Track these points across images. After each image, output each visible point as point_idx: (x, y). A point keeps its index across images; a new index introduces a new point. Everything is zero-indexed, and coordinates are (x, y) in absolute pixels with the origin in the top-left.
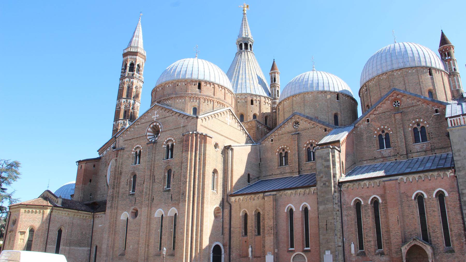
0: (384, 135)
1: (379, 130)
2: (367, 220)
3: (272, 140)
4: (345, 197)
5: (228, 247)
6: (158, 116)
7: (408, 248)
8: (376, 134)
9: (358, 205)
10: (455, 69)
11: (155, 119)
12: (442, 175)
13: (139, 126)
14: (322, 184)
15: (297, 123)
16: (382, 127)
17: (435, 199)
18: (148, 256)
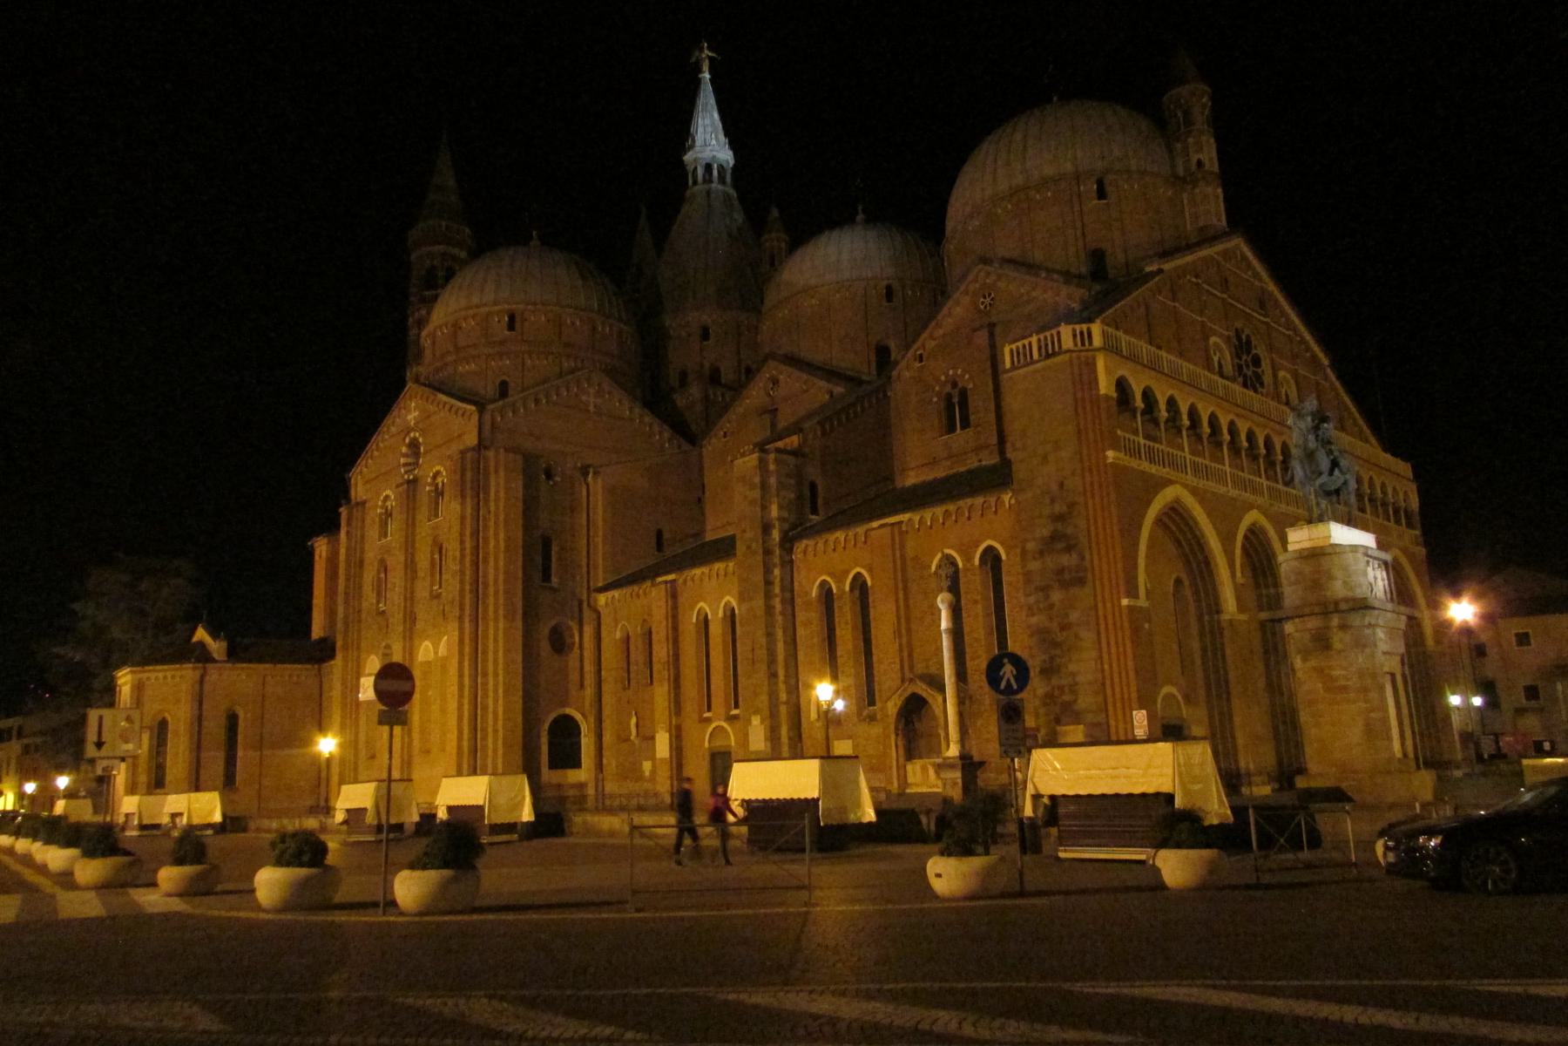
0: (956, 393)
1: (946, 382)
2: (844, 632)
3: (725, 435)
4: (800, 578)
5: (592, 719)
6: (417, 413)
7: (899, 703)
8: (939, 394)
9: (827, 596)
10: (1200, 164)
11: (412, 423)
12: (993, 504)
13: (386, 443)
14: (744, 548)
15: (775, 382)
16: (951, 372)
17: (977, 572)
18: (410, 756)
